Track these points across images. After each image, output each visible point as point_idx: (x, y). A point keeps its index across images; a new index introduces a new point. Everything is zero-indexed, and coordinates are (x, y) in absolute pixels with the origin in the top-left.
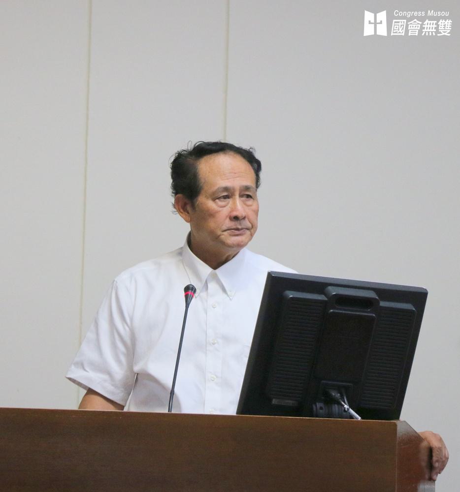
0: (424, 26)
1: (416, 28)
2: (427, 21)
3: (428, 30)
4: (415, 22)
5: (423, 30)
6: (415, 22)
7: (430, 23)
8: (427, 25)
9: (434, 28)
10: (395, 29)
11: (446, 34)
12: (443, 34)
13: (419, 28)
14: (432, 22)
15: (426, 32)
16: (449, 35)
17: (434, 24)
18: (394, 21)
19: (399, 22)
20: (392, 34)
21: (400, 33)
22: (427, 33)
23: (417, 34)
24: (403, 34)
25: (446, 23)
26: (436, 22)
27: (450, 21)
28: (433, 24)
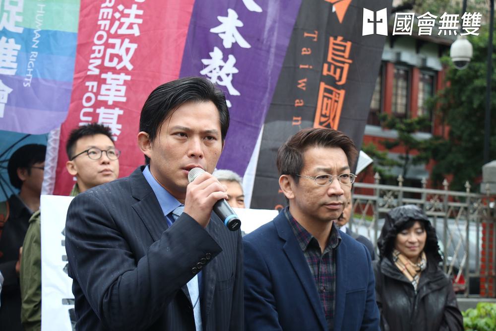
0: (440, 22)
1: (430, 24)
2: (445, 15)
3: (447, 28)
4: (428, 15)
5: (440, 28)
6: (428, 15)
7: (450, 17)
8: (446, 20)
9: (455, 25)
10: (398, 25)
11: (472, 33)
12: (469, 33)
13: (433, 25)
14: (452, 16)
15: (443, 30)
16: (477, 34)
17: (456, 18)
18: (397, 14)
19: (404, 16)
20: (394, 33)
21: (405, 31)
22: (445, 31)
23: (430, 34)
24: (410, 34)
25: (473, 17)
26: (458, 15)
27: (479, 15)
28: (454, 18)
